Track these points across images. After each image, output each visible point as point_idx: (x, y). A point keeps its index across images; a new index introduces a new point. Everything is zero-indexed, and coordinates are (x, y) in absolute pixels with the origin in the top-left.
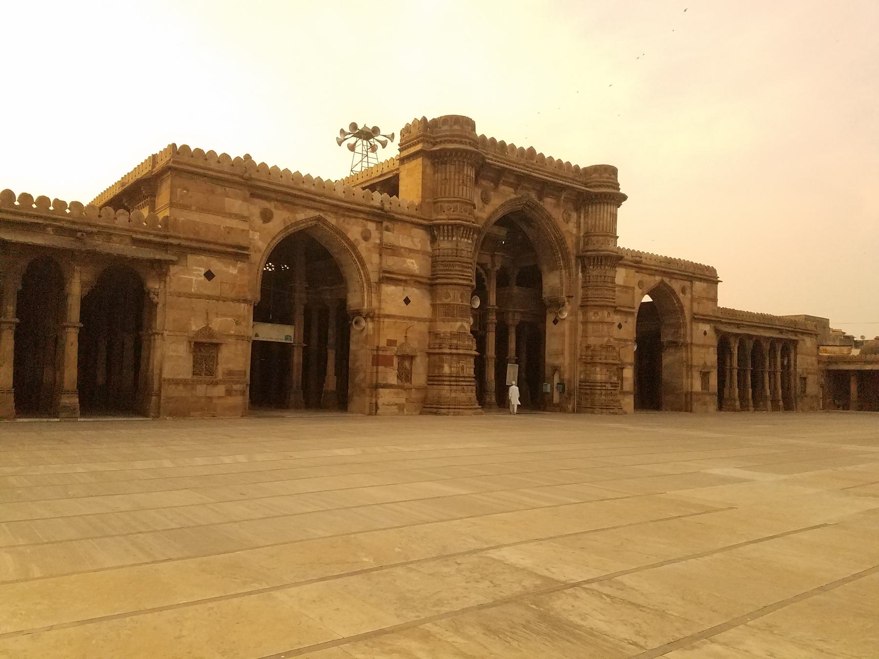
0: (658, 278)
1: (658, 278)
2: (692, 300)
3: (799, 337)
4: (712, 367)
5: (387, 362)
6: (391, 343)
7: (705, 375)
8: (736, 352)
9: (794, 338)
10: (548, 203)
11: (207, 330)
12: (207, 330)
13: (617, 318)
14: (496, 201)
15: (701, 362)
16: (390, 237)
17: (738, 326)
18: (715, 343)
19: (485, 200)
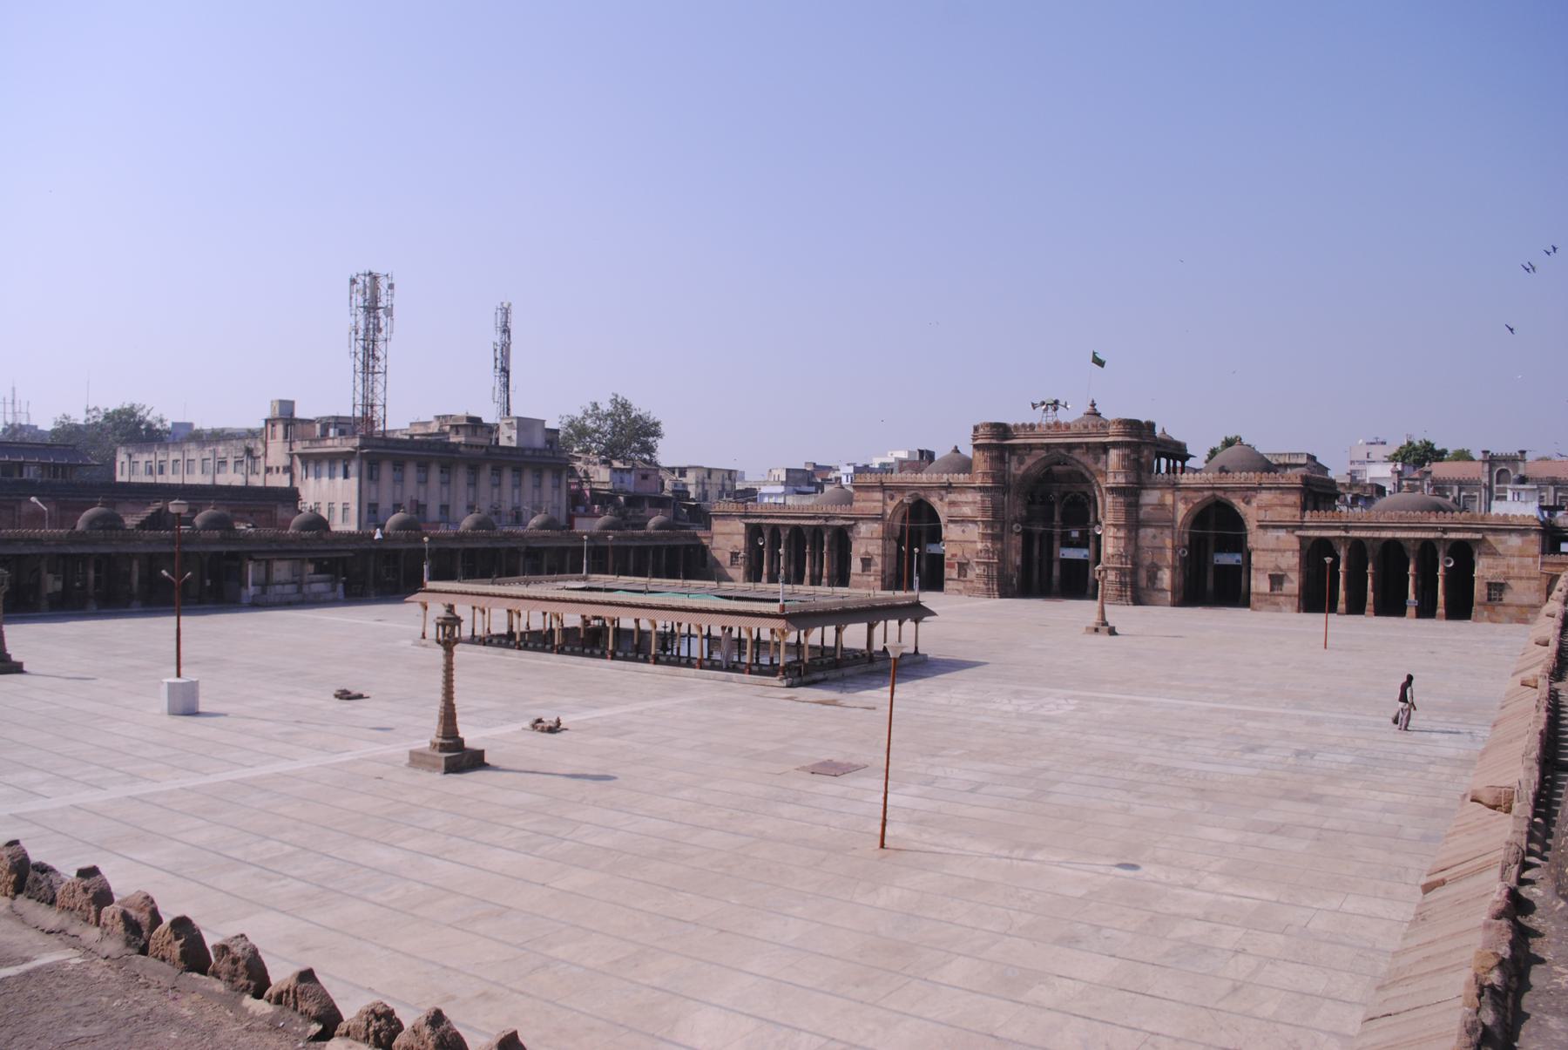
0: (1207, 493)
1: (1207, 493)
2: (1259, 507)
3: (1490, 537)
4: (1290, 569)
5: (951, 566)
6: (954, 555)
7: (1277, 580)
8: (1342, 553)
9: (1479, 536)
10: (1077, 454)
11: (867, 553)
12: (867, 553)
13: (1150, 531)
14: (1029, 461)
15: (1272, 565)
16: (953, 497)
17: (1346, 529)
18: (1297, 547)
19: (1021, 462)
